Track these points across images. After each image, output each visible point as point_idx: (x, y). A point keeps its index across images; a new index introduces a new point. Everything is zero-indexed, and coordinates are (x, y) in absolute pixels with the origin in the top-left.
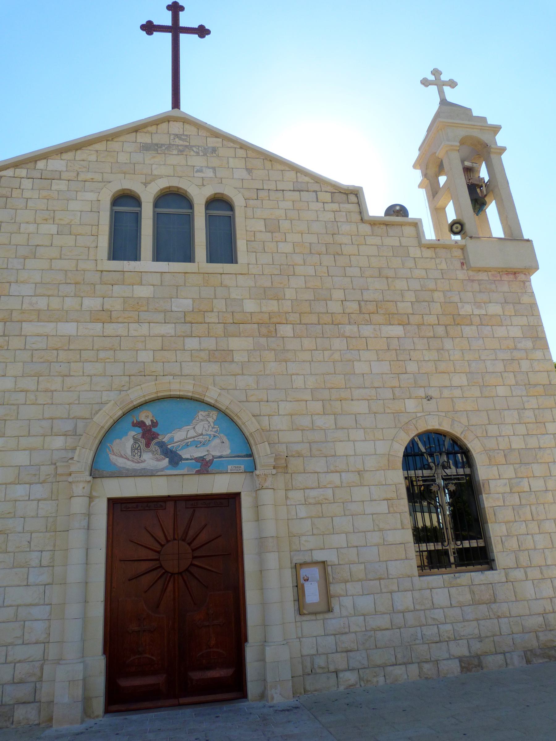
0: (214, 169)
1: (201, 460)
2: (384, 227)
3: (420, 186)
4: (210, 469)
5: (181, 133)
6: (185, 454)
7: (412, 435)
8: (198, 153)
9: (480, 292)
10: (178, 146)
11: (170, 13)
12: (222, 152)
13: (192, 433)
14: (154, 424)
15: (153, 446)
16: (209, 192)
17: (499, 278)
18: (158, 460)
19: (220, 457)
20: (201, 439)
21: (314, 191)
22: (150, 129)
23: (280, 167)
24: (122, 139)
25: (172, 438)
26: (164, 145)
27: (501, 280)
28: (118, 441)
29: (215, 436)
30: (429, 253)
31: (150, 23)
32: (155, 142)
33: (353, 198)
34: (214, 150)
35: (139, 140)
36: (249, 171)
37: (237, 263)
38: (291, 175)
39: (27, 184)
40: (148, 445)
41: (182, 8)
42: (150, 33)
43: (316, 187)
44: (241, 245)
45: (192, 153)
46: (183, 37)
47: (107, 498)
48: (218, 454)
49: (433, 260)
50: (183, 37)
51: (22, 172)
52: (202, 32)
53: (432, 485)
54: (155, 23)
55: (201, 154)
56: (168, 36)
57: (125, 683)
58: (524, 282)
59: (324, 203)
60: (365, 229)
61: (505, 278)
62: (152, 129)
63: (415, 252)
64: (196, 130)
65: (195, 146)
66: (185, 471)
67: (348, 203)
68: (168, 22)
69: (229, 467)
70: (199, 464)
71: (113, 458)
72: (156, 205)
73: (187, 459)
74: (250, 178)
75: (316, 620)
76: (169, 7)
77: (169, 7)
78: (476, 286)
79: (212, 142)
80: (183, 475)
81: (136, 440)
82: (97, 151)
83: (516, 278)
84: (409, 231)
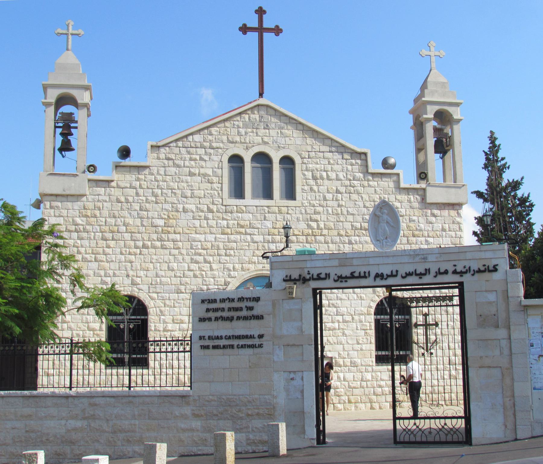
3: (411, 128)
7: (381, 298)
11: (257, 16)
16: (282, 153)
21: (341, 152)
23: (321, 136)
31: (245, 25)
33: (363, 157)
37: (295, 199)
41: (265, 12)
42: (245, 33)
43: (342, 150)
46: (265, 35)
50: (265, 35)
52: (277, 31)
54: (248, 26)
56: (256, 35)
64: (274, 112)
68: (256, 25)
76: (256, 12)
77: (256, 12)
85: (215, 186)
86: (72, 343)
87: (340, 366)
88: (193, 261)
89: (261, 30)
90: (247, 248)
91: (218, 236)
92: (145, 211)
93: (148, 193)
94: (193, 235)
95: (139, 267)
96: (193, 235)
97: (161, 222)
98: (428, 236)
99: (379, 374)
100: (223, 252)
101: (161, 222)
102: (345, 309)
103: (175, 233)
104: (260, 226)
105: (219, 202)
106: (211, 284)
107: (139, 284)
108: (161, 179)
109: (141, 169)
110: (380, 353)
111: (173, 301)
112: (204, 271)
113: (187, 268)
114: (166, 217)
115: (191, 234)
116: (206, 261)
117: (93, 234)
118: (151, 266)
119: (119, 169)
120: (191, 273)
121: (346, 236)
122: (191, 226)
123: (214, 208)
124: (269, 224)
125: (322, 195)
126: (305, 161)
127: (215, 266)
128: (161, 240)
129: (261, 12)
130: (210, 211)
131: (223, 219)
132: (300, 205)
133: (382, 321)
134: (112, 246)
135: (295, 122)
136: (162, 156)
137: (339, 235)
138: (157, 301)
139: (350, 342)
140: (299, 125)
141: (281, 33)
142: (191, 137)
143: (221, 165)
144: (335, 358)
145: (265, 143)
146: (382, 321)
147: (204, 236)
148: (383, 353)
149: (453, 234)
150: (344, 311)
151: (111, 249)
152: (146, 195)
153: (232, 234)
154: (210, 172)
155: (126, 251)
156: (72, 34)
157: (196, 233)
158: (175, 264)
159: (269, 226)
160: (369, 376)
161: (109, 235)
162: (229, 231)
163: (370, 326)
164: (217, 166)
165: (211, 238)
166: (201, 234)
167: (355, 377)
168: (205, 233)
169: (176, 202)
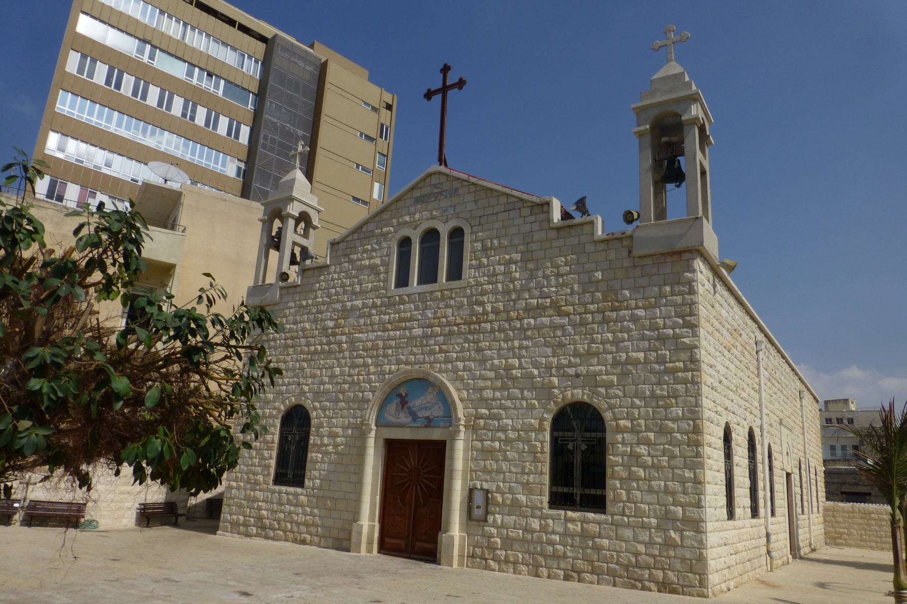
0: (454, 206)
1: (427, 418)
2: (568, 230)
4: (432, 424)
5: (438, 182)
6: (421, 414)
8: (446, 197)
9: (642, 276)
10: (435, 193)
11: (441, 75)
12: (461, 191)
13: (424, 402)
14: (407, 395)
15: (405, 409)
17: (662, 260)
18: (407, 417)
19: (437, 417)
20: (428, 405)
22: (420, 185)
24: (405, 197)
25: (414, 404)
26: (426, 195)
27: (665, 262)
28: (389, 405)
29: (436, 403)
30: (602, 247)
32: (423, 193)
34: (456, 190)
35: (414, 196)
36: (476, 201)
38: (503, 200)
39: (358, 243)
40: (402, 408)
43: (520, 205)
44: (466, 263)
45: (443, 197)
47: (384, 439)
48: (436, 415)
49: (605, 253)
51: (356, 236)
53: (568, 444)
55: (448, 196)
57: (387, 540)
58: (688, 260)
59: (524, 217)
60: (553, 234)
61: (669, 259)
62: (421, 185)
63: (590, 248)
65: (444, 191)
66: (418, 425)
67: (543, 213)
69: (441, 424)
70: (426, 421)
71: (386, 415)
72: (422, 242)
73: (420, 418)
74: (476, 208)
75: (479, 525)
78: (638, 272)
79: (456, 184)
80: (418, 427)
81: (397, 405)
82: (392, 210)
83: (681, 257)
84: (587, 229)
85: (382, 276)
86: (534, 462)
87: (498, 504)
88: (354, 366)
89: (444, 90)
90: (404, 345)
91: (379, 333)
92: (320, 314)
93: (324, 293)
94: (357, 335)
95: (309, 374)
96: (357, 335)
97: (331, 324)
98: (637, 307)
99: (550, 522)
100: (381, 352)
101: (331, 324)
102: (510, 422)
103: (342, 334)
104: (420, 317)
105: (383, 293)
106: (367, 390)
107: (307, 393)
108: (337, 277)
109: (322, 269)
110: (599, 492)
111: (331, 411)
112: (362, 375)
113: (347, 373)
114: (336, 317)
115: (355, 333)
116: (366, 365)
117: (279, 341)
118: (318, 372)
119: (307, 273)
120: (349, 379)
121: (517, 319)
122: (356, 324)
123: (378, 302)
124: (430, 314)
125: (492, 268)
126: (475, 229)
127: (372, 369)
128: (329, 343)
129: (446, 69)
130: (374, 306)
131: (385, 314)
132: (466, 285)
133: (561, 441)
134: (291, 353)
135: (466, 183)
136: (340, 253)
137: (509, 320)
138: (319, 411)
139: (513, 469)
140: (471, 186)
141: (464, 84)
142: (366, 226)
143: (389, 251)
144: (492, 493)
145: (433, 218)
146: (561, 441)
147: (366, 335)
148: (593, 492)
149: (679, 299)
150: (508, 425)
151: (290, 357)
152: (323, 296)
153: (392, 330)
154: (378, 261)
155: (300, 357)
156: (300, 153)
157: (360, 333)
158: (338, 369)
159: (430, 315)
160: (535, 524)
161: (289, 342)
162: (389, 326)
163: (542, 447)
164: (385, 253)
165: (372, 336)
166: (365, 333)
167: (517, 522)
168: (367, 332)
169: (346, 299)
